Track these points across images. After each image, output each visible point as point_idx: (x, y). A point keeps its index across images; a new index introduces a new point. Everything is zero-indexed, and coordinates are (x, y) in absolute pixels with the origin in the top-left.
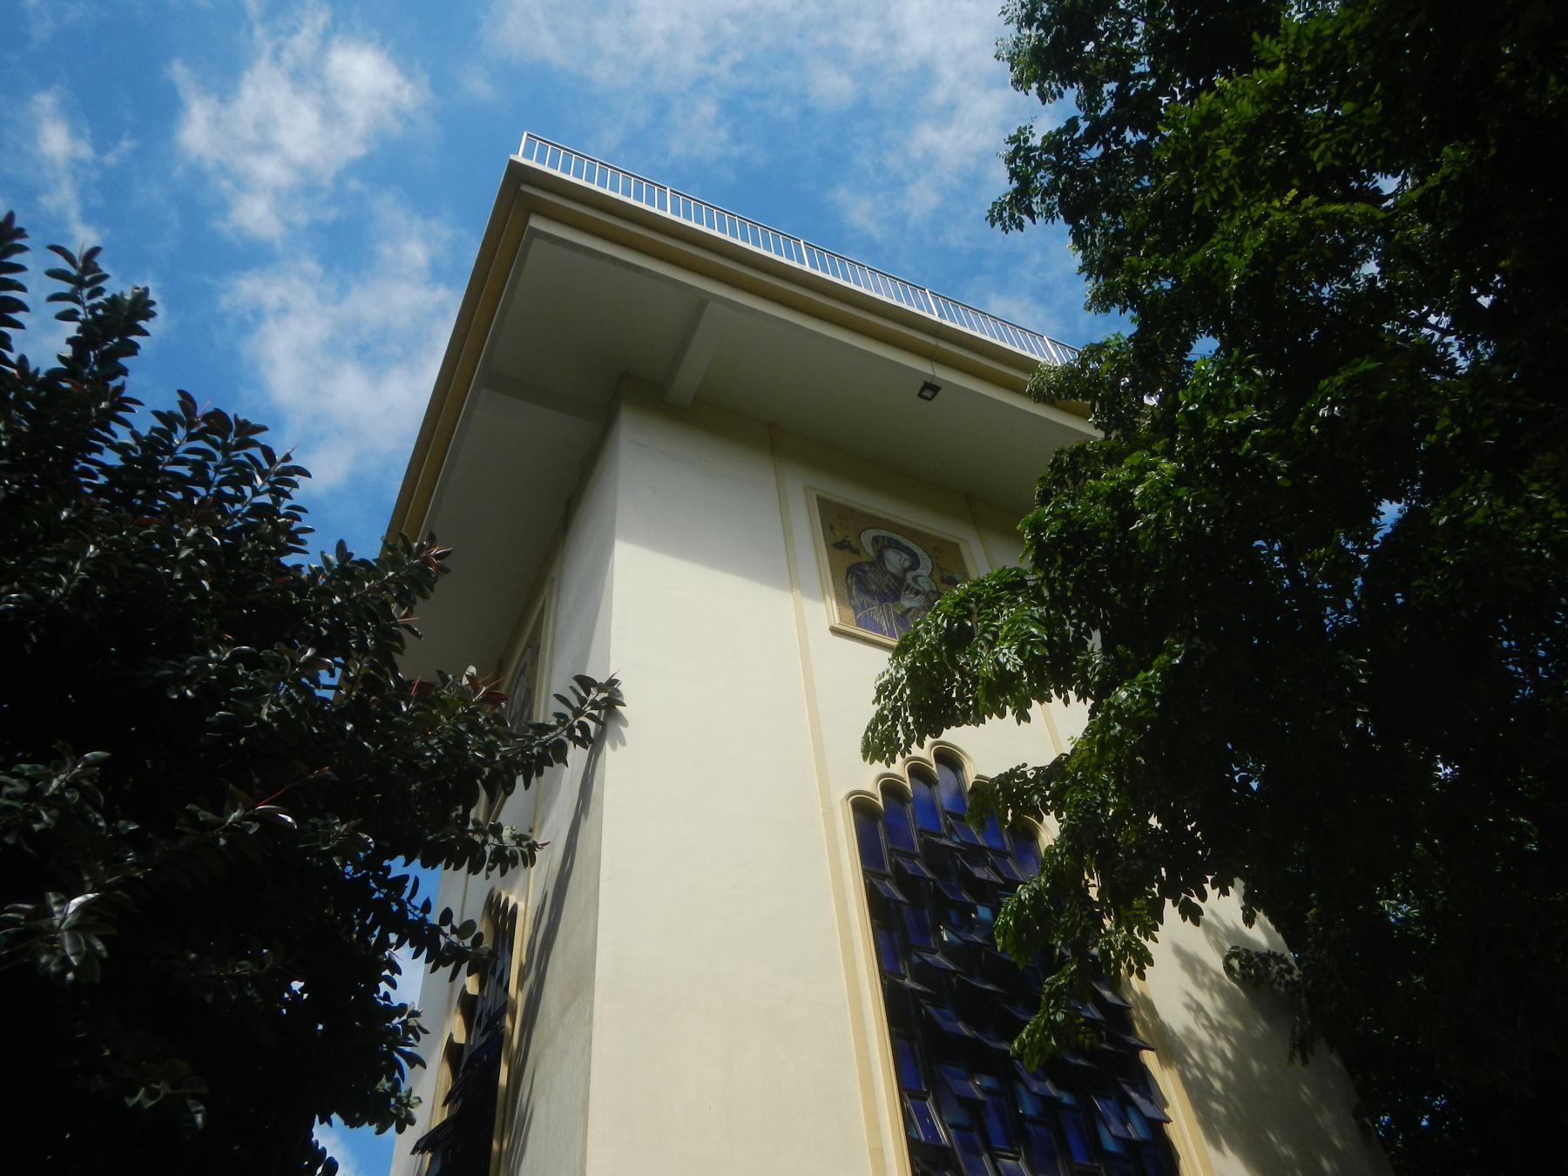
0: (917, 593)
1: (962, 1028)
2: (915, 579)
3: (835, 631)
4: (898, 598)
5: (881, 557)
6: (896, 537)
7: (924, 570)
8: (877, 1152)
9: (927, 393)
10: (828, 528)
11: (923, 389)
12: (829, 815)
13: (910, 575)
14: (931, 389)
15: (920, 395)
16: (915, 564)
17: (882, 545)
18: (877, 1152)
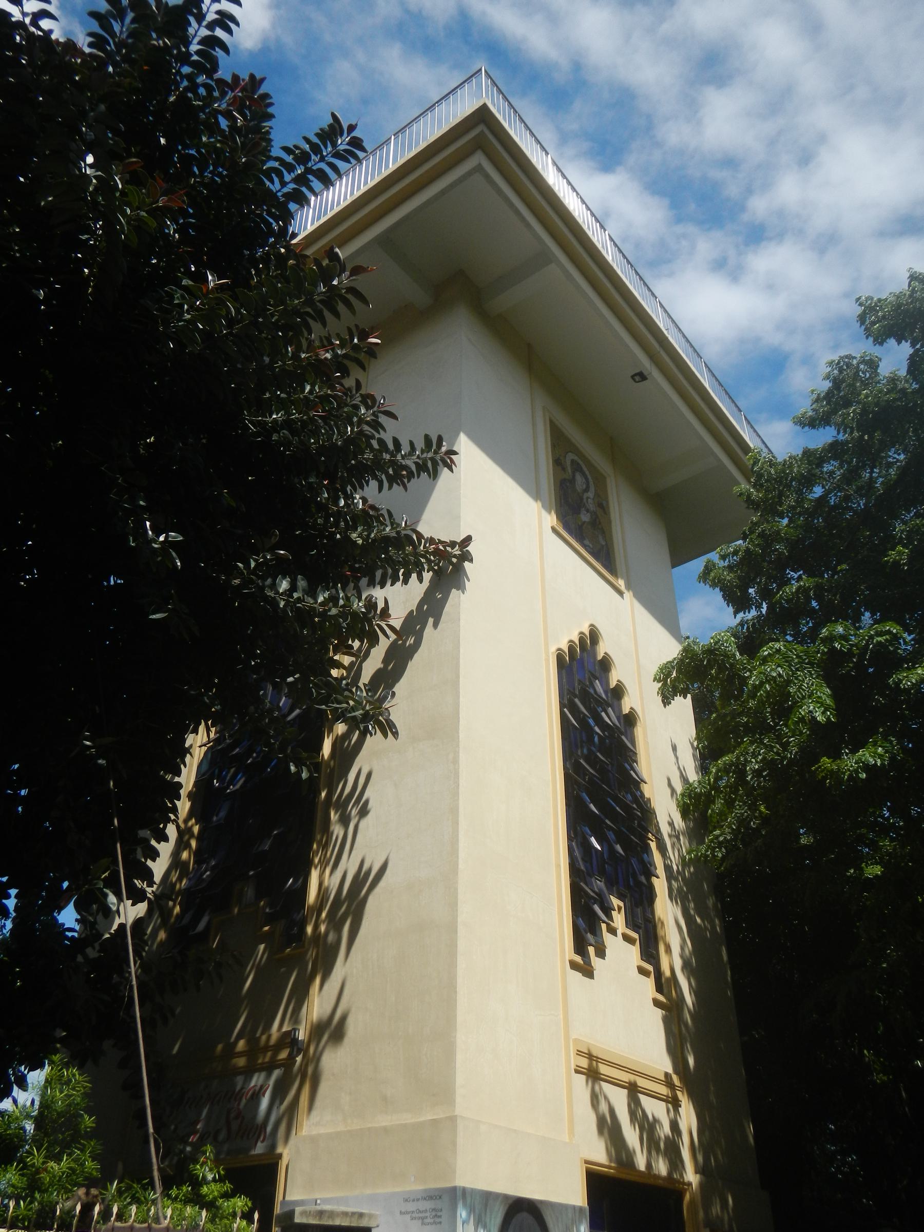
0: (588, 511)
1: (592, 807)
2: (588, 498)
3: (554, 530)
4: (579, 513)
5: (574, 476)
6: (581, 463)
7: (591, 494)
8: (558, 866)
9: (637, 378)
10: (554, 446)
11: (636, 375)
12: (547, 660)
13: (586, 495)
14: (641, 376)
15: (633, 377)
16: (587, 490)
17: (576, 467)
18: (558, 866)
